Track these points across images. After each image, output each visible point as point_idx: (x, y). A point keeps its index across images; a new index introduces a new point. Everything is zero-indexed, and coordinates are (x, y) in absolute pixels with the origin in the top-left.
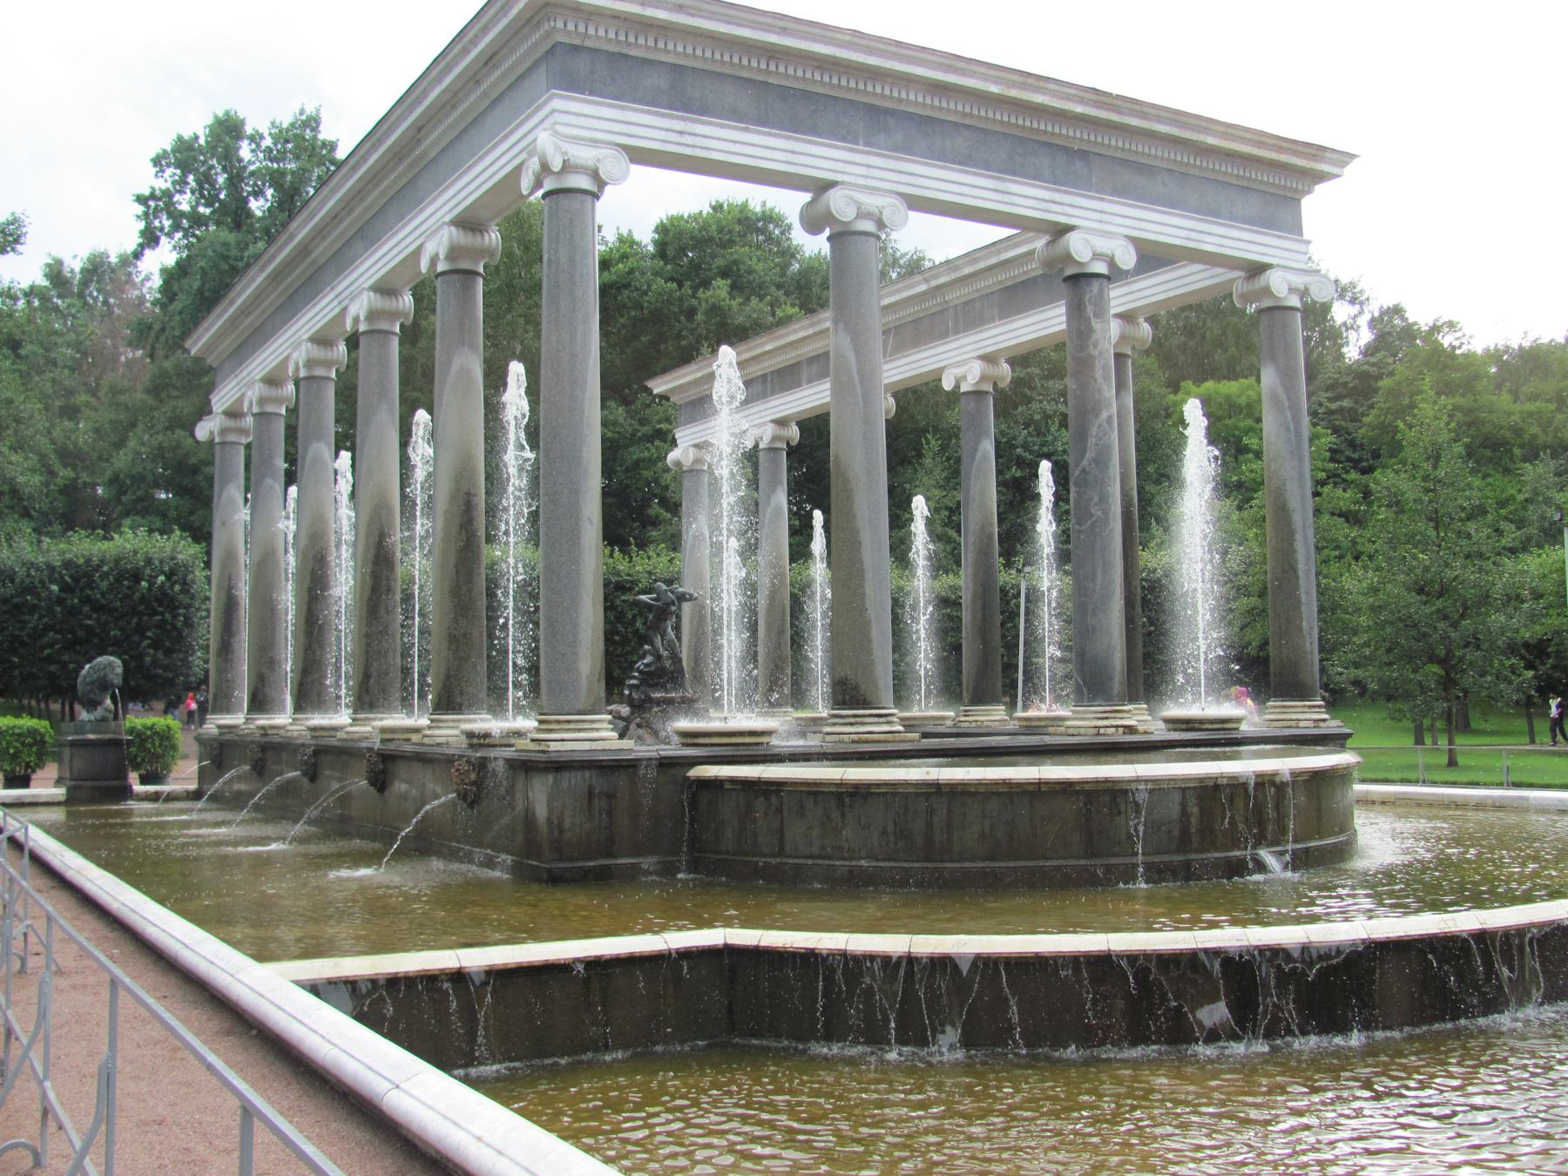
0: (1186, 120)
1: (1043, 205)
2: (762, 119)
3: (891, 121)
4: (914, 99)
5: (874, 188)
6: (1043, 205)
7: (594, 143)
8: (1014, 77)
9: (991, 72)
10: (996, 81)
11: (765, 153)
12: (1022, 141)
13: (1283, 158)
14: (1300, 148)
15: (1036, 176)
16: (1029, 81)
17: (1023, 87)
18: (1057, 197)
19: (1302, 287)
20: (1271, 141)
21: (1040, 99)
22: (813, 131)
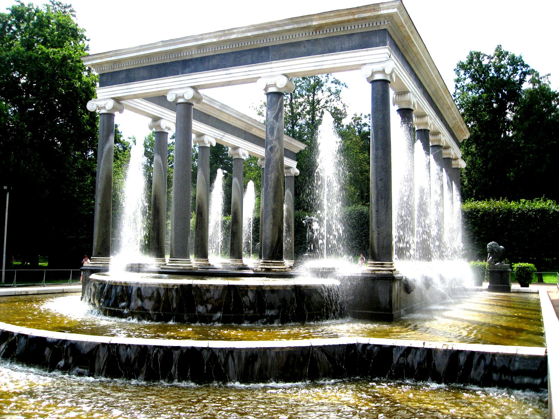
0: (298, 20)
1: (246, 73)
2: (151, 77)
3: (191, 63)
4: (196, 54)
5: (181, 88)
6: (246, 73)
7: (105, 99)
9: (211, 35)
10: (215, 37)
12: (239, 52)
13: (356, 16)
14: (364, 9)
15: (245, 63)
16: (226, 32)
17: (225, 35)
18: (251, 68)
19: (381, 69)
20: (345, 12)
21: (233, 37)
22: (165, 75)
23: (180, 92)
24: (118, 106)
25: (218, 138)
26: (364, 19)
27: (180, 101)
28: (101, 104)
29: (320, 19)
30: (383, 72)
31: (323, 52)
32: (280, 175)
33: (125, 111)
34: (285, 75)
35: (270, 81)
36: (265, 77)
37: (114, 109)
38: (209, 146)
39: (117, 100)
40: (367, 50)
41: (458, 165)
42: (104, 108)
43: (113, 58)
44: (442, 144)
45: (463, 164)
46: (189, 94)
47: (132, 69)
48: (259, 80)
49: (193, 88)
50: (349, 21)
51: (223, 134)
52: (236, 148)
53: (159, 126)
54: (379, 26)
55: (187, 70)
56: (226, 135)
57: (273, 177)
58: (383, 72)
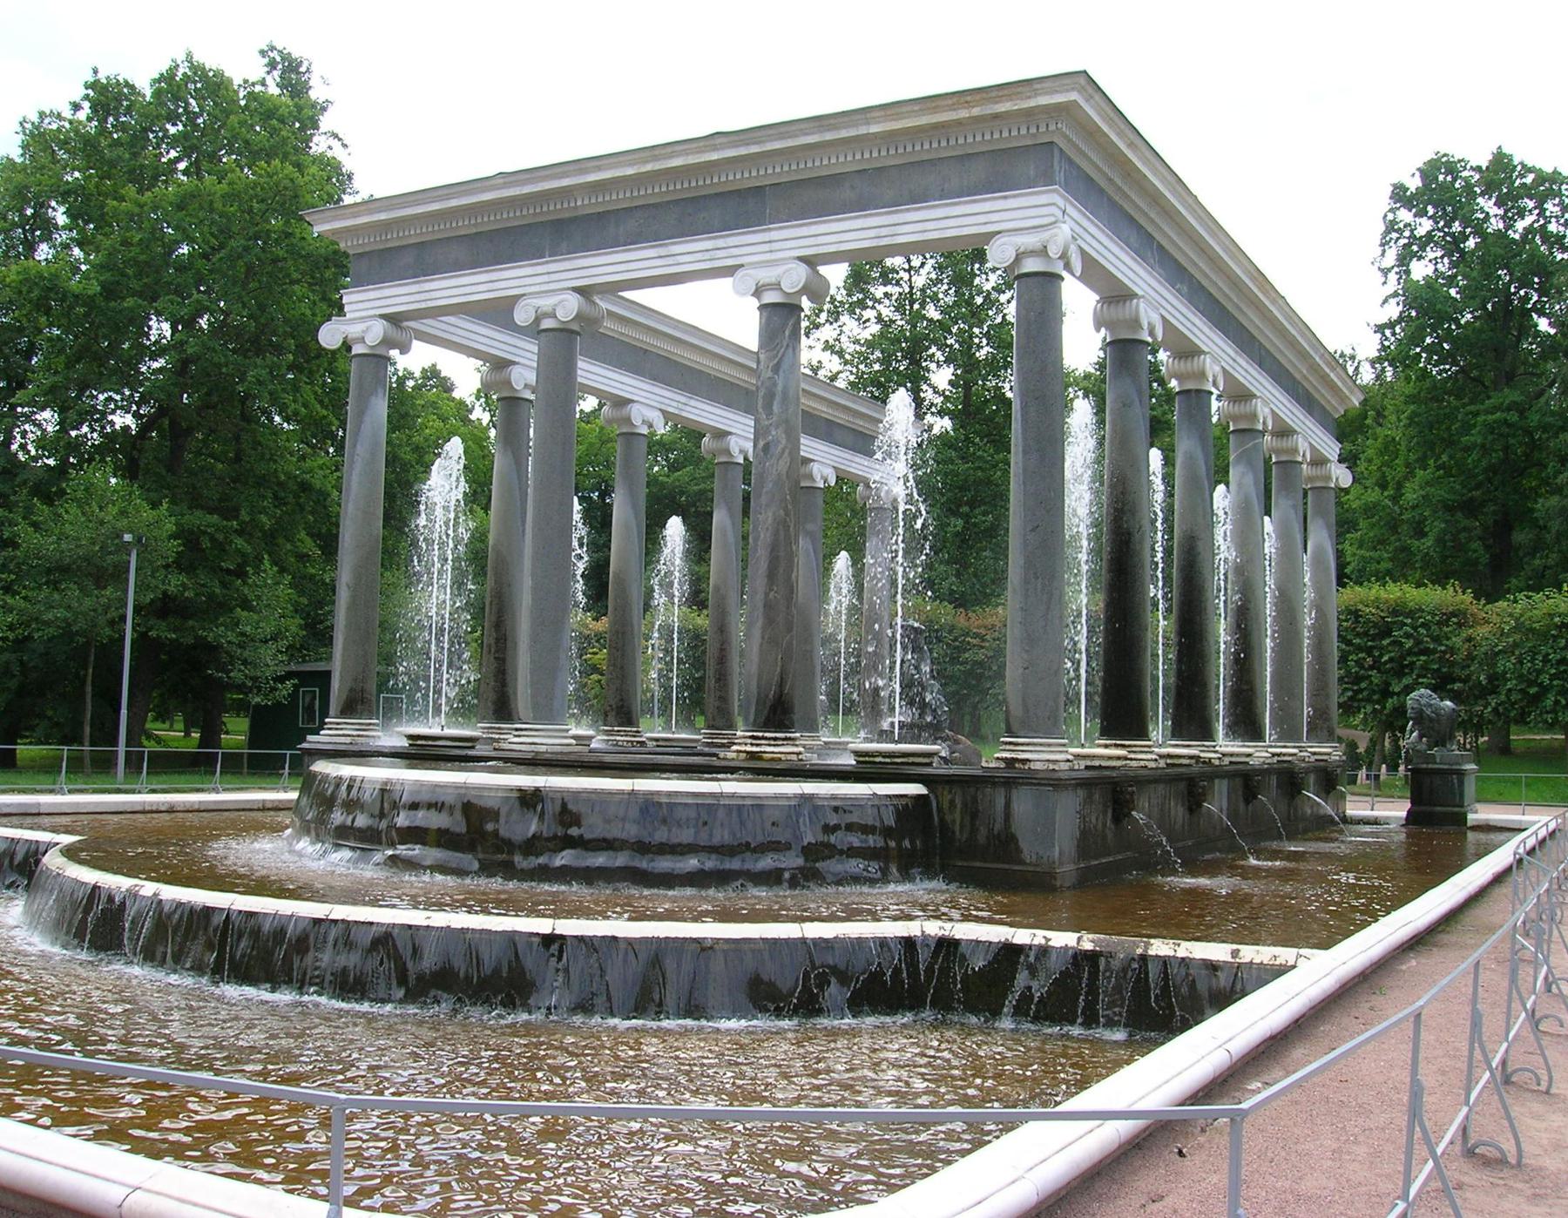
1: (707, 256)
2: (475, 263)
8: (643, 155)
11: (474, 289)
13: (976, 111)
15: (707, 229)
18: (720, 243)
19: (1038, 246)
23: (546, 303)
24: (395, 334)
25: (671, 410)
26: (996, 116)
27: (547, 324)
28: (354, 330)
29: (887, 118)
30: (1043, 252)
31: (896, 203)
32: (787, 514)
33: (415, 343)
34: (801, 259)
35: (766, 275)
36: (755, 265)
37: (388, 343)
38: (645, 431)
39: (394, 319)
40: (1005, 197)
41: (1329, 478)
42: (362, 340)
43: (383, 216)
44: (1260, 427)
45: (1342, 476)
46: (568, 307)
47: (431, 242)
48: (740, 273)
49: (581, 291)
50: (959, 123)
51: (683, 399)
52: (721, 435)
53: (508, 383)
54: (1034, 135)
55: (564, 245)
56: (692, 403)
57: (770, 520)
58: (1043, 252)
